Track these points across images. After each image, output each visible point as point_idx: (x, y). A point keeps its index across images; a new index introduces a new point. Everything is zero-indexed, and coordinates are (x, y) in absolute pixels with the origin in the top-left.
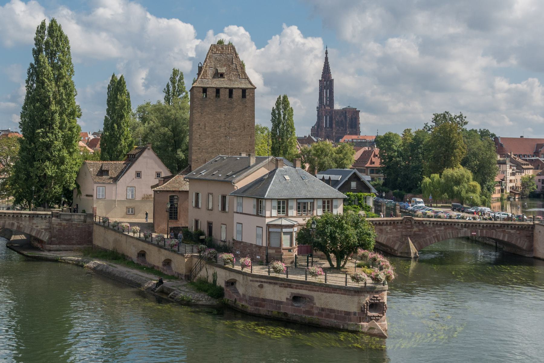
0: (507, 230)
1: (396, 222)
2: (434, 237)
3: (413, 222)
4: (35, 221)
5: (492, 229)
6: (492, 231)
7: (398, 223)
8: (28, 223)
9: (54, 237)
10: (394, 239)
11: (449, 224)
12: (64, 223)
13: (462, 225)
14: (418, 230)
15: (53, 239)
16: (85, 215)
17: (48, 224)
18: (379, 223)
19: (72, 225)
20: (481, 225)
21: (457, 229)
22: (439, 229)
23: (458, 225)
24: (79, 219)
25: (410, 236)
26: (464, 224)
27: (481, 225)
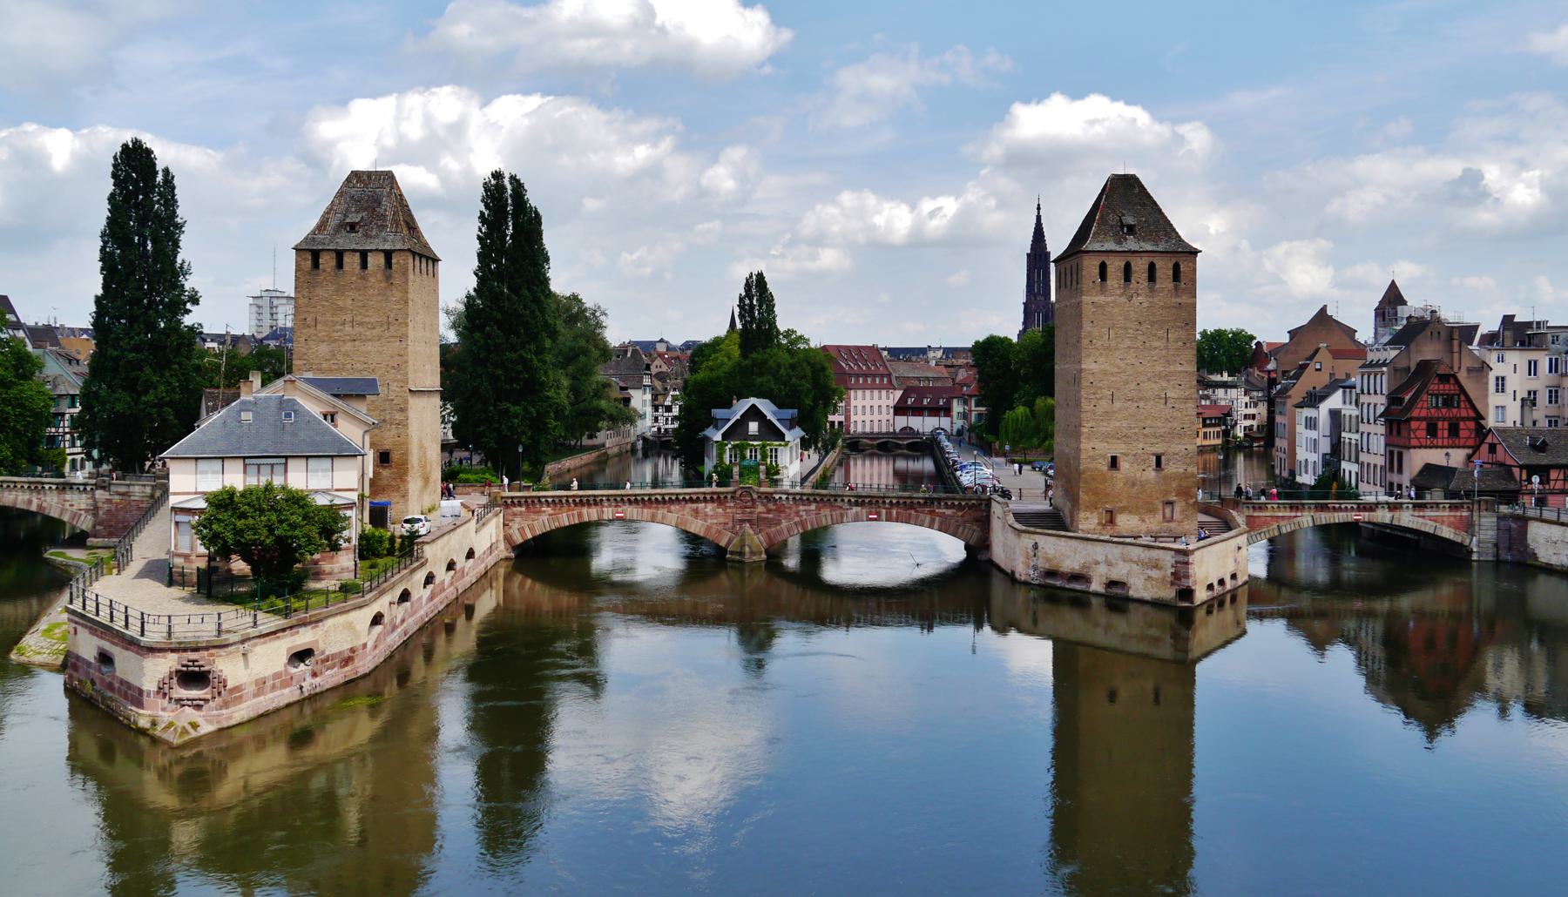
0: (937, 511)
1: (722, 496)
2: (795, 523)
3: (755, 496)
4: (68, 497)
6: (908, 512)
7: (726, 497)
8: (55, 499)
9: (100, 524)
10: (720, 528)
11: (825, 499)
12: (116, 498)
13: (849, 501)
14: (765, 510)
15: (98, 528)
16: (152, 486)
17: (90, 501)
18: (691, 498)
19: (129, 503)
20: (888, 501)
21: (841, 508)
22: (806, 508)
23: (843, 500)
24: (143, 492)
25: (749, 521)
26: (853, 500)
27: (888, 501)
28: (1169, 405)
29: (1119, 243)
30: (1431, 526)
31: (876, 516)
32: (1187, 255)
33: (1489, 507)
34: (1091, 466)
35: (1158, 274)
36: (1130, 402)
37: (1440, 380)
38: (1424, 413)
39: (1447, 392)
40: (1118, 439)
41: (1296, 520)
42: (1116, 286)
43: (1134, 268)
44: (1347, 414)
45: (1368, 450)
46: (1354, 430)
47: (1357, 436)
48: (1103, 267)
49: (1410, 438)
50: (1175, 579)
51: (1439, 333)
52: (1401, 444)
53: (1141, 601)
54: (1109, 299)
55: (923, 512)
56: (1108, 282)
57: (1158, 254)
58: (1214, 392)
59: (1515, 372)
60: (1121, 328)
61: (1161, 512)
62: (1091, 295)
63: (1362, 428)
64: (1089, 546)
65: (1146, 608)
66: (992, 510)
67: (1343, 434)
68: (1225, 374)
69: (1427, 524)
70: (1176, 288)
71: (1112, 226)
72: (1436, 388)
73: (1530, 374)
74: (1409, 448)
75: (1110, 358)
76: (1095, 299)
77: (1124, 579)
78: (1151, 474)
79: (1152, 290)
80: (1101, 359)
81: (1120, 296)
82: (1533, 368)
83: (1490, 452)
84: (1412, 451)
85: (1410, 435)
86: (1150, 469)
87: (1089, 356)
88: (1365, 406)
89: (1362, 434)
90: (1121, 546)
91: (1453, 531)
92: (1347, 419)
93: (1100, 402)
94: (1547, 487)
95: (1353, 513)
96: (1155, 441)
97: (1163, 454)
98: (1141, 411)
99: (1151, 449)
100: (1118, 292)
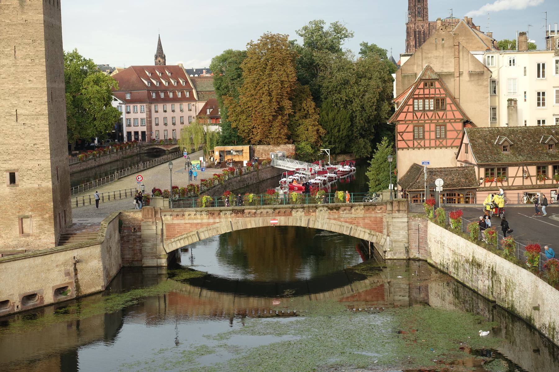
33: (401, 209)
37: (425, 85)
39: (431, 96)
41: (214, 226)
59: (525, 75)
61: (17, 228)
72: (421, 92)
73: (539, 76)
78: (5, 189)
82: (541, 69)
83: (466, 153)
86: (5, 185)
91: (368, 231)
94: (505, 184)
96: (8, 158)
97: (17, 170)
99: (4, 165)
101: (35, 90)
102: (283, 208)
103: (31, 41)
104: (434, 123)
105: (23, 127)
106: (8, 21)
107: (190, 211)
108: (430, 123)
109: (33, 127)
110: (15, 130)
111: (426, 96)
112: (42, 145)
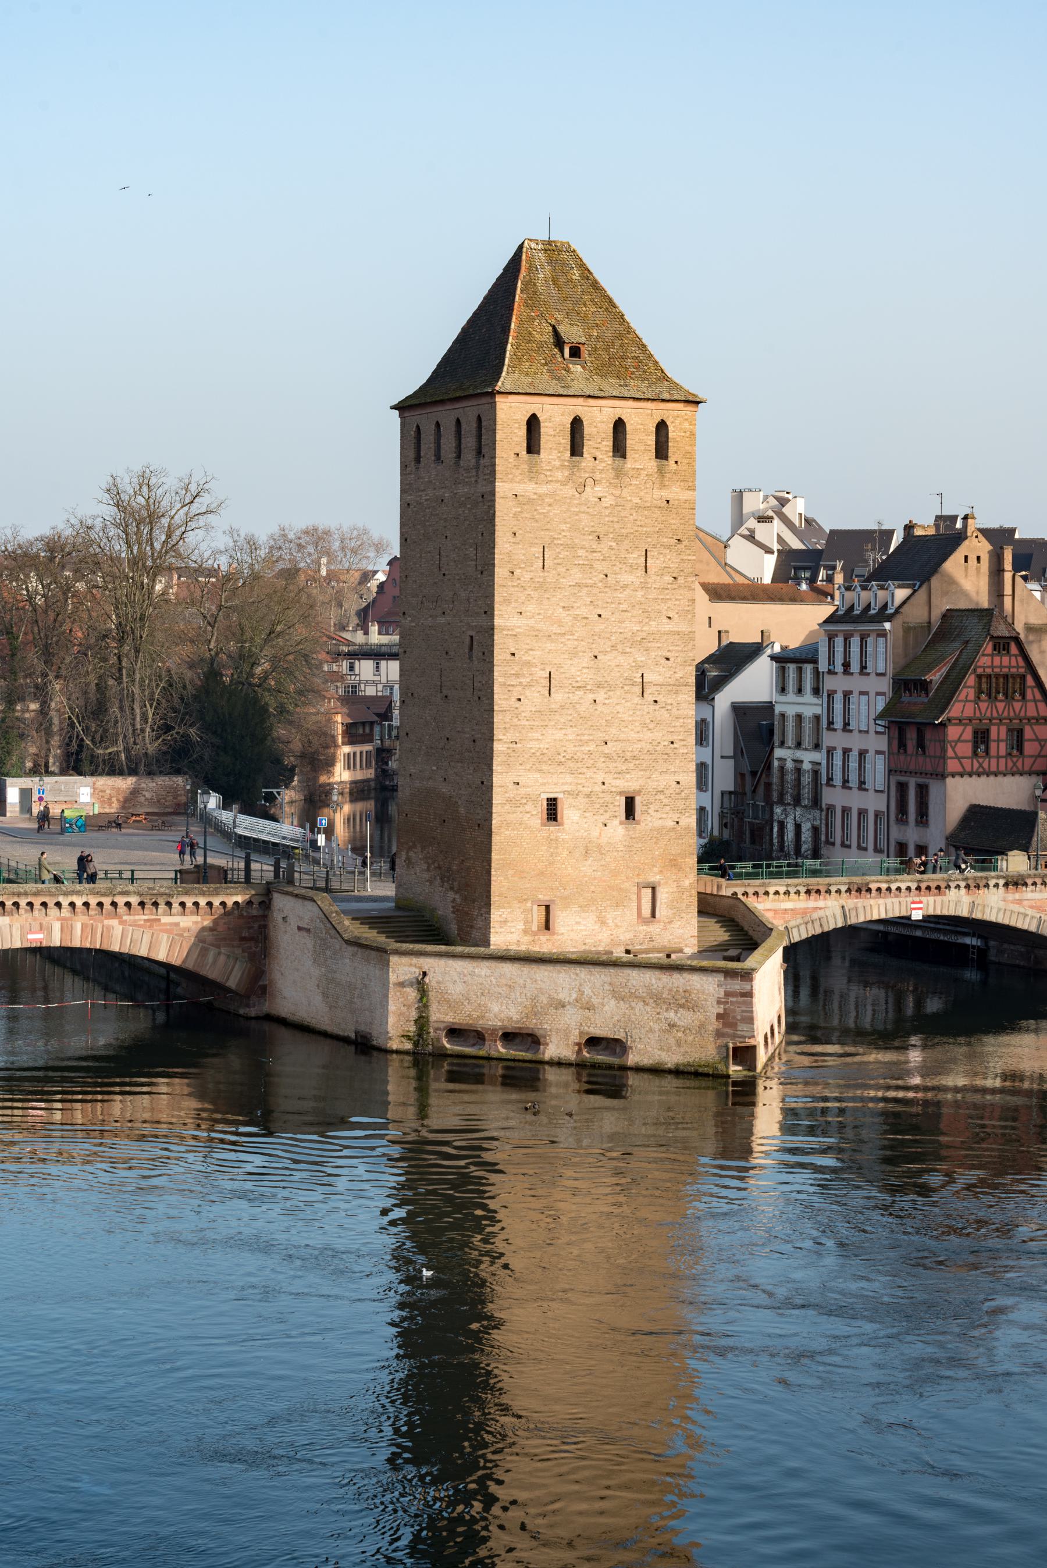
5: (109, 917)
6: (106, 922)
28: (649, 698)
29: (559, 379)
30: (1033, 917)
31: (40, 936)
32: (681, 406)
34: (512, 817)
35: (629, 442)
36: (580, 693)
38: (969, 711)
40: (560, 763)
42: (557, 463)
43: (588, 430)
44: (791, 711)
45: (846, 781)
46: (807, 740)
47: (819, 756)
48: (533, 424)
49: (943, 757)
50: (725, 1025)
51: (978, 558)
52: (929, 768)
53: (656, 1071)
54: (543, 489)
55: (134, 924)
56: (542, 455)
57: (631, 403)
58: (352, 668)
60: (566, 546)
62: (512, 481)
63: (828, 739)
64: (542, 973)
65: (670, 1083)
66: (277, 916)
67: (779, 753)
68: (374, 629)
69: (1026, 915)
70: (661, 471)
71: (541, 345)
74: (942, 776)
75: (545, 602)
76: (519, 488)
77: (620, 1035)
78: (617, 830)
79: (619, 473)
80: (530, 608)
81: (564, 483)
84: (949, 780)
85: (944, 750)
86: (616, 822)
87: (507, 601)
88: (839, 697)
89: (828, 752)
90: (612, 971)
92: (791, 724)
93: (528, 693)
95: (910, 899)
96: (624, 768)
97: (639, 792)
98: (600, 708)
99: (618, 782)
100: (560, 475)
101: (676, 637)
102: (933, 880)
103: (673, 541)
104: (1005, 724)
105: (652, 707)
106: (636, 500)
107: (776, 885)
108: (998, 725)
109: (669, 707)
110: (638, 713)
111: (996, 670)
112: (683, 743)
